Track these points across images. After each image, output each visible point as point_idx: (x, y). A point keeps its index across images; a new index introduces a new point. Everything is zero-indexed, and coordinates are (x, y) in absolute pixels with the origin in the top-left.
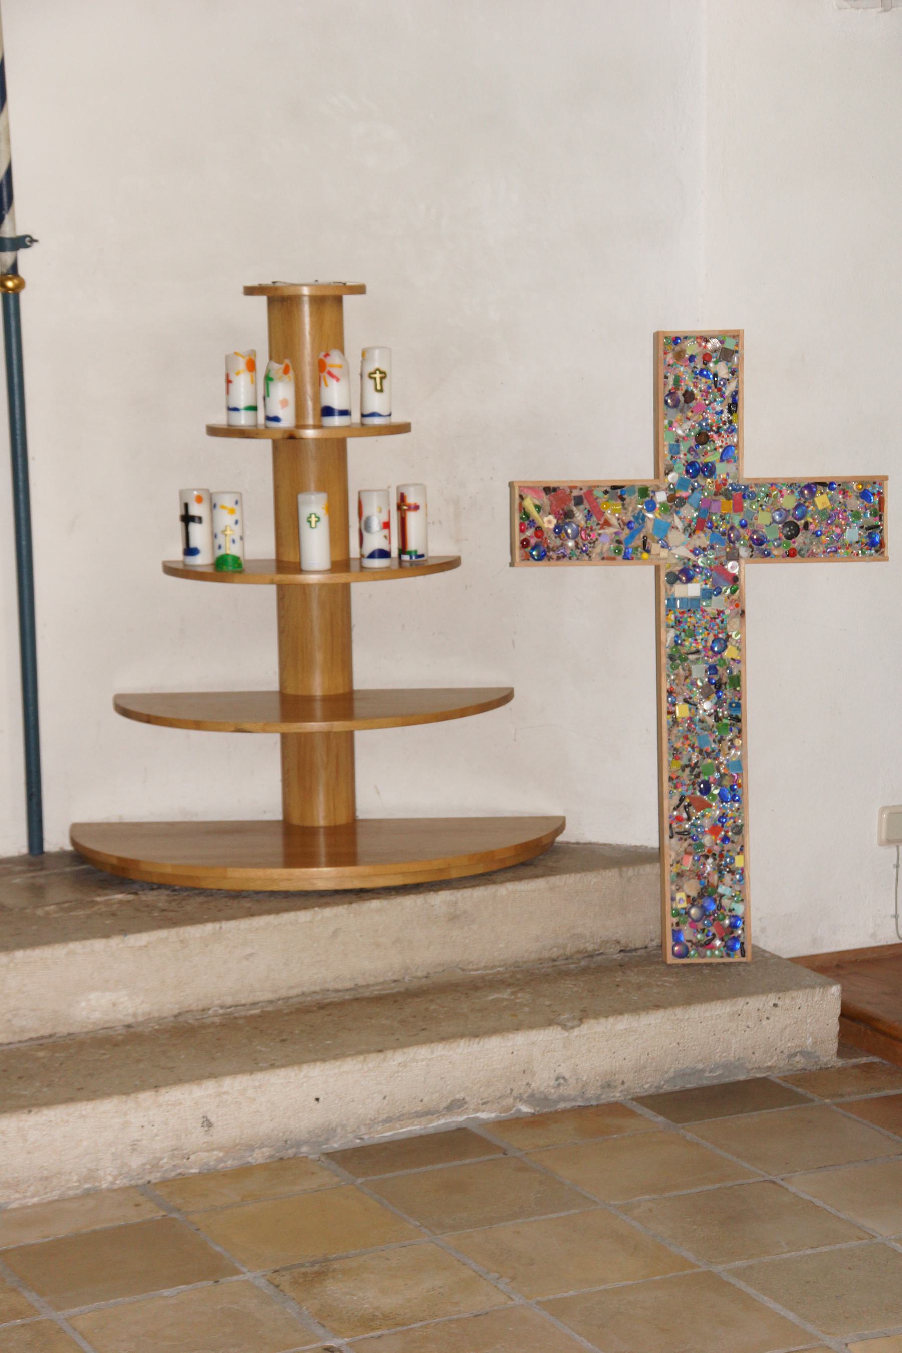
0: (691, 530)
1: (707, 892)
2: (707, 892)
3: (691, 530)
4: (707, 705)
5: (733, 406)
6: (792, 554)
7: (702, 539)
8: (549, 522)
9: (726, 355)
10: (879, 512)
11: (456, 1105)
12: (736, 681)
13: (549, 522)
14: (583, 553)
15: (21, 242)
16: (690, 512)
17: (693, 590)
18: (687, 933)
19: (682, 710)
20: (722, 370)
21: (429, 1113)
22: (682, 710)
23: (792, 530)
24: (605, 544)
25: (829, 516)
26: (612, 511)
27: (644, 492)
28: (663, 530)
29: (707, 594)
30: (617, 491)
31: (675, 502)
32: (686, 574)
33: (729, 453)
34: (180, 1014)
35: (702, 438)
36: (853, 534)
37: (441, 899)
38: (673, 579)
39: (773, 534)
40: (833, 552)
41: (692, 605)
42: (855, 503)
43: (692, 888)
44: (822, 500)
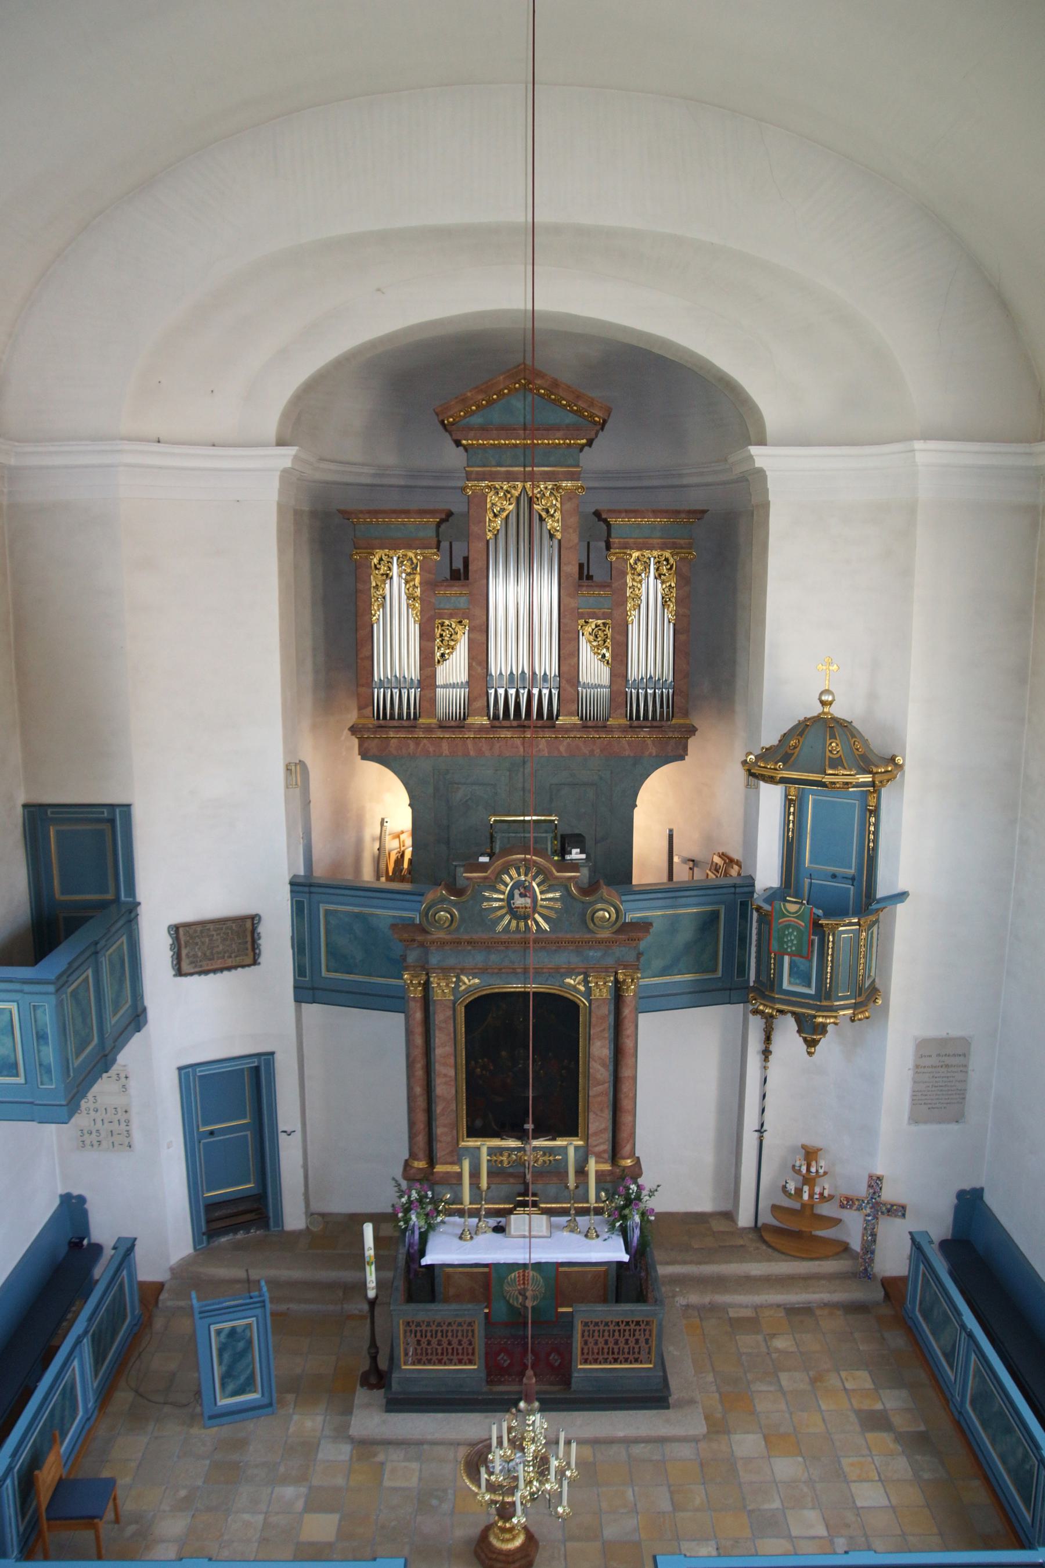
0: (871, 1208)
1: (866, 1269)
2: (866, 1269)
3: (871, 1208)
4: (870, 1238)
5: (881, 1189)
6: (888, 1215)
7: (873, 1210)
8: (845, 1202)
9: (880, 1180)
10: (905, 1211)
11: (810, 1303)
12: (876, 1235)
13: (845, 1202)
14: (851, 1208)
15: (765, 1131)
16: (871, 1205)
17: (870, 1218)
18: (861, 1274)
19: (865, 1238)
20: (879, 1183)
21: (805, 1304)
22: (865, 1238)
23: (889, 1211)
24: (855, 1207)
25: (896, 1210)
26: (857, 1203)
27: (863, 1201)
28: (866, 1207)
29: (872, 1220)
30: (857, 1200)
31: (868, 1203)
32: (869, 1215)
33: (879, 1196)
34: (769, 1276)
35: (874, 1193)
36: (900, 1214)
37: (817, 1263)
38: (866, 1216)
39: (886, 1211)
40: (896, 1216)
41: (869, 1221)
42: (901, 1209)
43: (863, 1268)
44: (895, 1207)
